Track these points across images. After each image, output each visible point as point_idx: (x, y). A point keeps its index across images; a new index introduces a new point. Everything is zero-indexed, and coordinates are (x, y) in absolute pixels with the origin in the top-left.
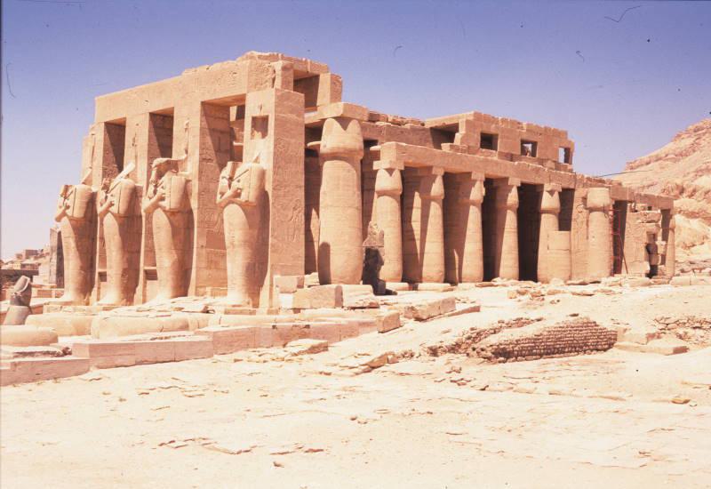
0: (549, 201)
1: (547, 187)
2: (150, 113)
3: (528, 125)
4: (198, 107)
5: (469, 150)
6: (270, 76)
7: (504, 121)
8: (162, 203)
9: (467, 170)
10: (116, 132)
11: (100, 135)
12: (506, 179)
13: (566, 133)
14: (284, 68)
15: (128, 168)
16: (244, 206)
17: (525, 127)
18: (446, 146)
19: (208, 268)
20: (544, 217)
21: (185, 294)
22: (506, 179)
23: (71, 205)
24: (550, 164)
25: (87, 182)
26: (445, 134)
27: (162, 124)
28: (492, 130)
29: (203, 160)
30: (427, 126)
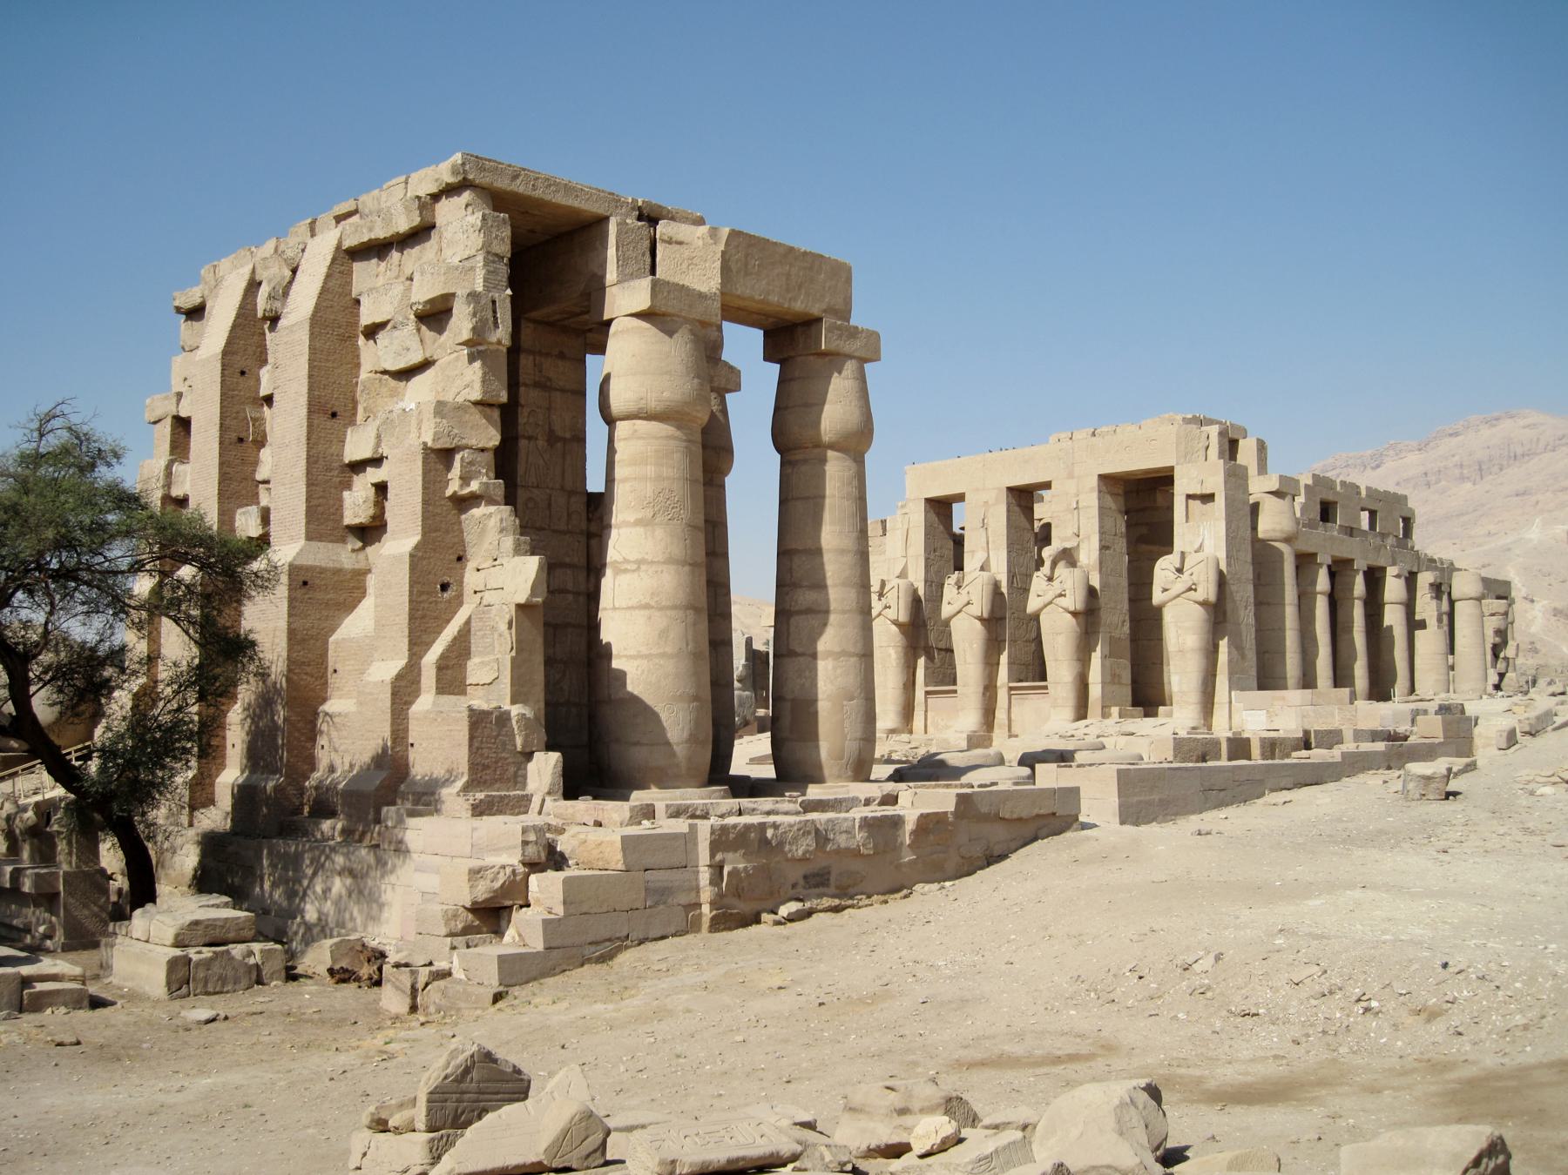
1: (1391, 571)
2: (1010, 489)
3: (1368, 489)
4: (1094, 481)
5: (1311, 525)
6: (1203, 443)
7: (1343, 483)
8: (1063, 602)
9: (1312, 550)
11: (917, 517)
12: (1351, 561)
13: (1405, 497)
14: (1221, 434)
15: (971, 562)
16: (1204, 604)
17: (1364, 493)
19: (1113, 682)
20: (1387, 608)
21: (1085, 717)
22: (1351, 561)
23: (893, 604)
24: (1390, 541)
25: (903, 574)
27: (1023, 497)
29: (1104, 548)
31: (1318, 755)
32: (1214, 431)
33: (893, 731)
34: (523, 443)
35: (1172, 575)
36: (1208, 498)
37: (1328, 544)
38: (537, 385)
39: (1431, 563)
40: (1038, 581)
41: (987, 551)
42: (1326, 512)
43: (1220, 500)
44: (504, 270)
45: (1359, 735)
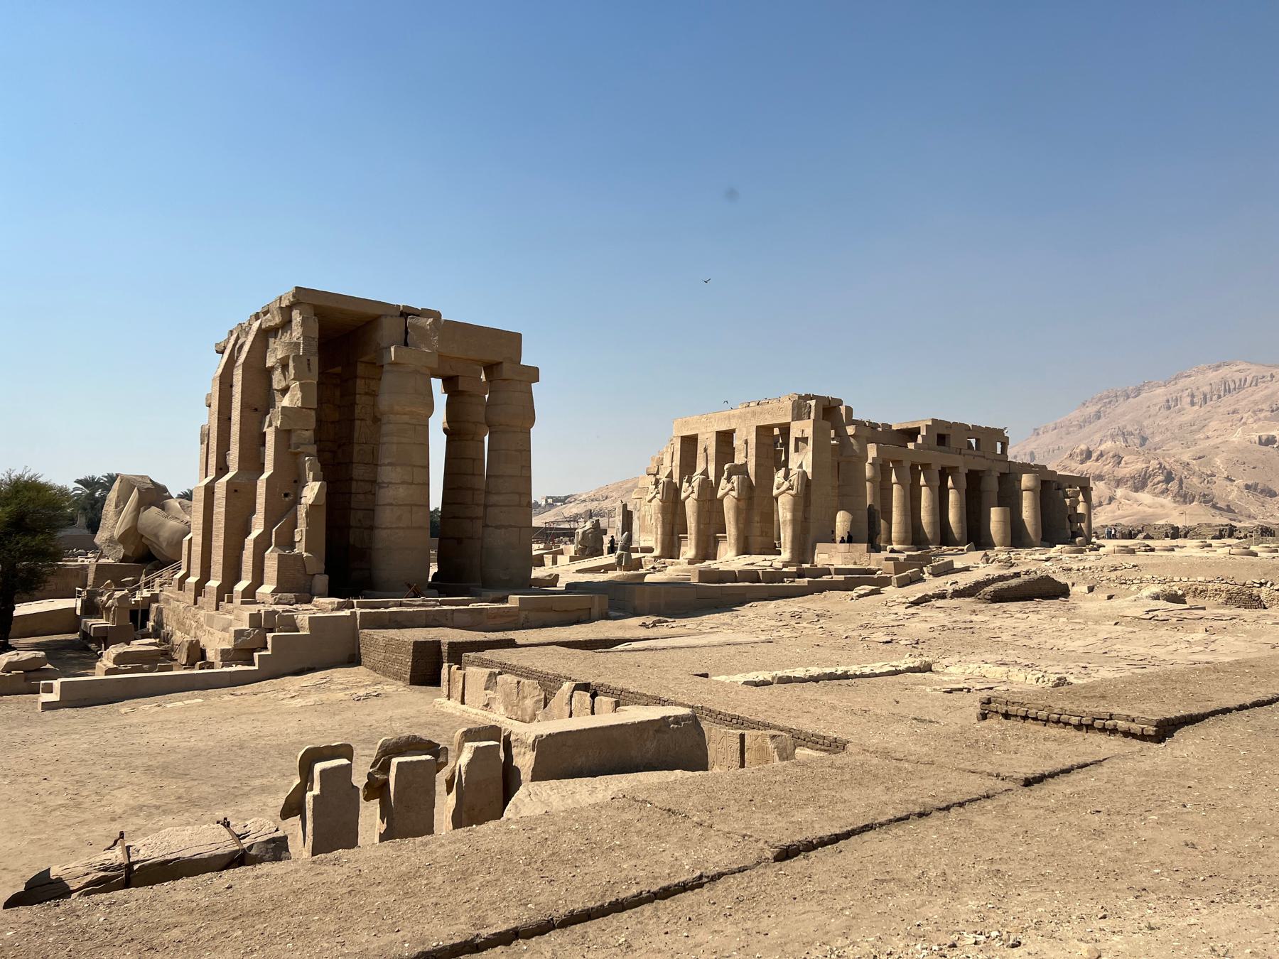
0: (992, 485)
10: (689, 443)
18: (911, 446)
26: (912, 434)
27: (725, 439)
28: (945, 432)
30: (894, 428)
31: (804, 581)
32: (813, 403)
33: (660, 557)
34: (357, 423)
35: (782, 480)
36: (805, 440)
37: (939, 459)
38: (366, 394)
39: (1027, 468)
40: (723, 482)
41: (705, 463)
42: (942, 439)
43: (810, 442)
44: (315, 344)
45: (838, 571)
